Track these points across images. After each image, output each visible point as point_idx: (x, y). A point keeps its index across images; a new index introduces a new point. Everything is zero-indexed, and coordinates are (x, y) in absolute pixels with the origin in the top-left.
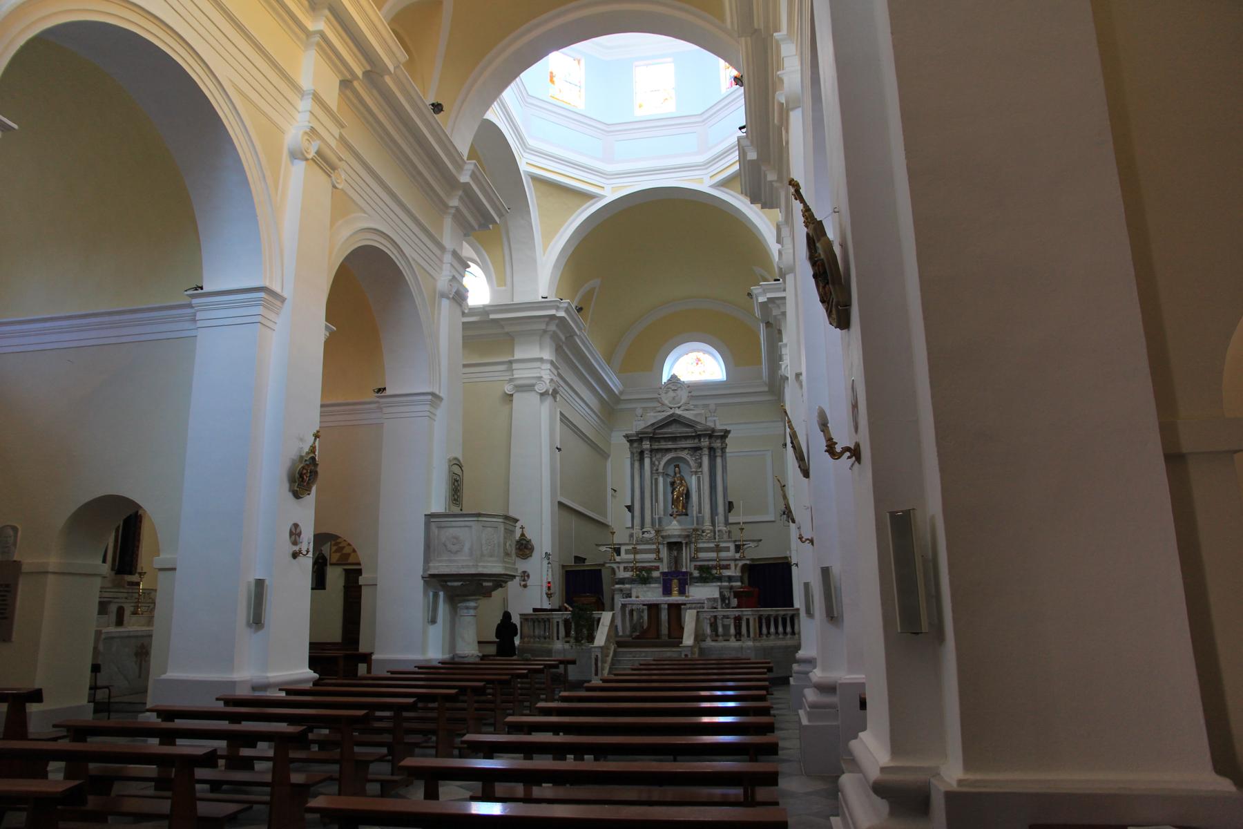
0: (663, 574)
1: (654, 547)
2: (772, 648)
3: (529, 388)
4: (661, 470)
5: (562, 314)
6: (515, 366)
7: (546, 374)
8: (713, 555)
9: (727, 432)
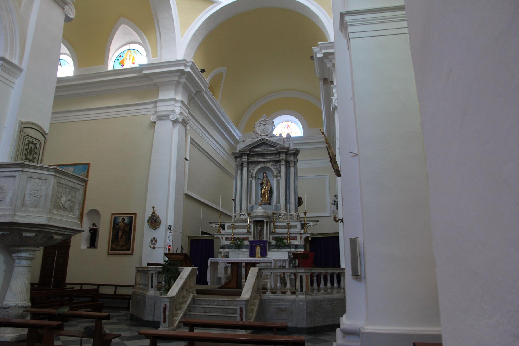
0: (250, 242)
1: (246, 224)
2: (321, 301)
3: (164, 117)
5: (188, 70)
6: (158, 104)
7: (178, 108)
8: (285, 230)
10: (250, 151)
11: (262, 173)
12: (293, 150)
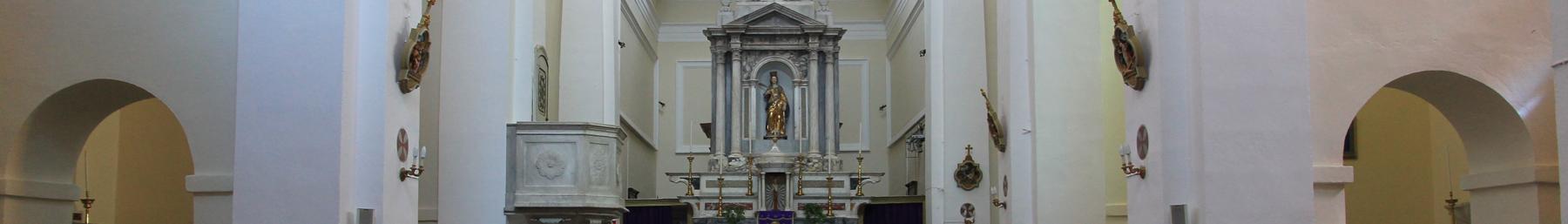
1: (745, 178)
4: (753, 77)
8: (824, 191)
9: (842, 32)
10: (747, 29)
11: (767, 74)
12: (835, 30)
